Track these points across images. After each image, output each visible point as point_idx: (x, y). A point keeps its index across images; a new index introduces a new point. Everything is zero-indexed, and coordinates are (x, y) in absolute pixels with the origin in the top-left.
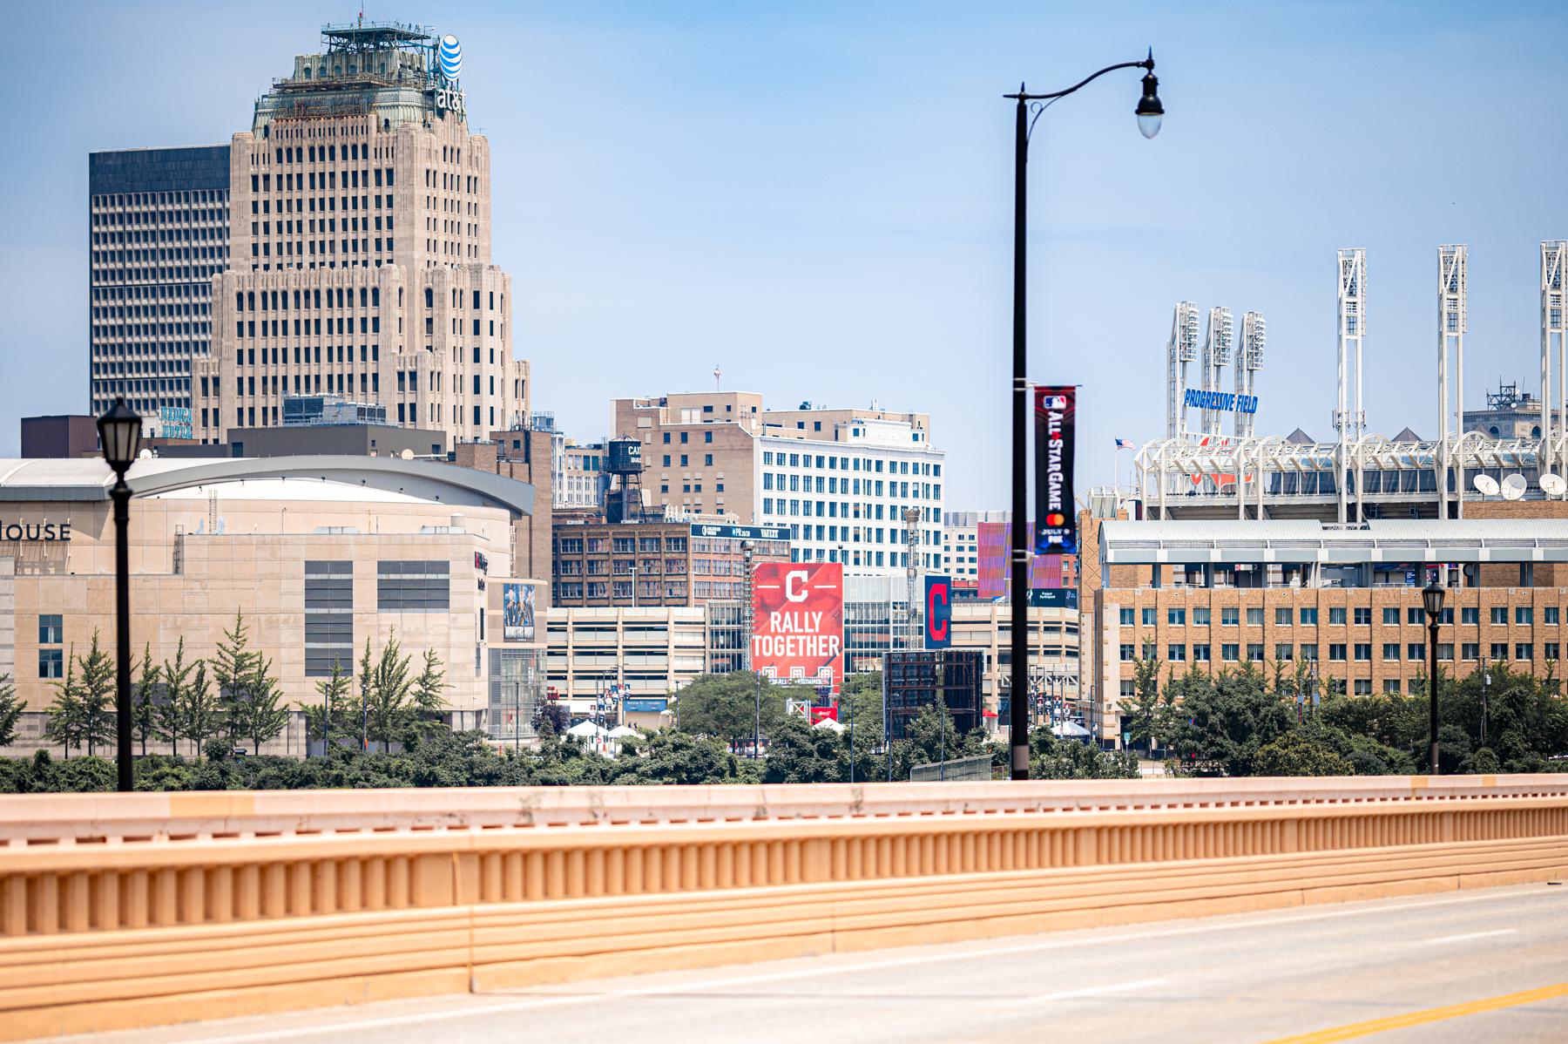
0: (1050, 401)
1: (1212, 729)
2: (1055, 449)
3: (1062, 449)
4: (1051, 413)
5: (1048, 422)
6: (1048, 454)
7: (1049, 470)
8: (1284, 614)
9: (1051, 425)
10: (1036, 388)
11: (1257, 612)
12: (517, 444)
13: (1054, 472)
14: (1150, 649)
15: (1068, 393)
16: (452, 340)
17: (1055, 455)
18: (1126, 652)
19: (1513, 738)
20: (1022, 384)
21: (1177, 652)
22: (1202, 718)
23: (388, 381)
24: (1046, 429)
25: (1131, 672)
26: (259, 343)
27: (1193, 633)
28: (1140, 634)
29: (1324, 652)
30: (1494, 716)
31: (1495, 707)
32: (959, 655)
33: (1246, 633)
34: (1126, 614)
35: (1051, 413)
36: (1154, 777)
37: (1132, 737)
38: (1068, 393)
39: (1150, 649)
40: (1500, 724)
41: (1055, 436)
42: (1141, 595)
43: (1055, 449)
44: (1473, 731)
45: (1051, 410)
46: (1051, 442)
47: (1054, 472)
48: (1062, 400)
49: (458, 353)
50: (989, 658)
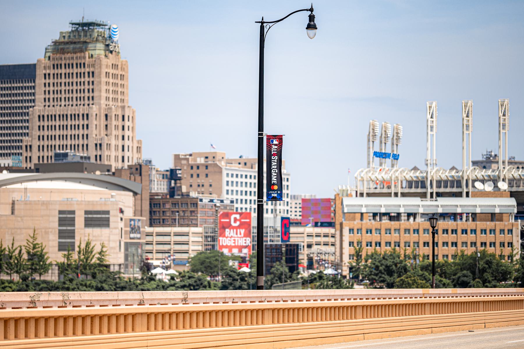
0: (273, 142)
1: (381, 272)
2: (275, 160)
8: (407, 231)
10: (267, 136)
11: (398, 230)
12: (137, 169)
13: (274, 169)
14: (359, 243)
15: (280, 138)
16: (114, 132)
17: (275, 162)
18: (351, 244)
19: (487, 276)
20: (262, 134)
21: (369, 244)
22: (377, 268)
23: (92, 147)
24: (271, 152)
25: (353, 252)
26: (46, 133)
27: (375, 237)
28: (356, 237)
29: (421, 244)
30: (481, 267)
31: (481, 264)
32: (291, 245)
33: (394, 237)
34: (351, 230)
35: (273, 146)
36: (359, 290)
37: (353, 275)
38: (280, 138)
39: (359, 243)
40: (483, 271)
41: (274, 155)
42: (356, 223)
43: (275, 160)
44: (473, 273)
45: (273, 145)
46: (273, 157)
47: (274, 169)
48: (277, 141)
49: (117, 137)
50: (303, 246)
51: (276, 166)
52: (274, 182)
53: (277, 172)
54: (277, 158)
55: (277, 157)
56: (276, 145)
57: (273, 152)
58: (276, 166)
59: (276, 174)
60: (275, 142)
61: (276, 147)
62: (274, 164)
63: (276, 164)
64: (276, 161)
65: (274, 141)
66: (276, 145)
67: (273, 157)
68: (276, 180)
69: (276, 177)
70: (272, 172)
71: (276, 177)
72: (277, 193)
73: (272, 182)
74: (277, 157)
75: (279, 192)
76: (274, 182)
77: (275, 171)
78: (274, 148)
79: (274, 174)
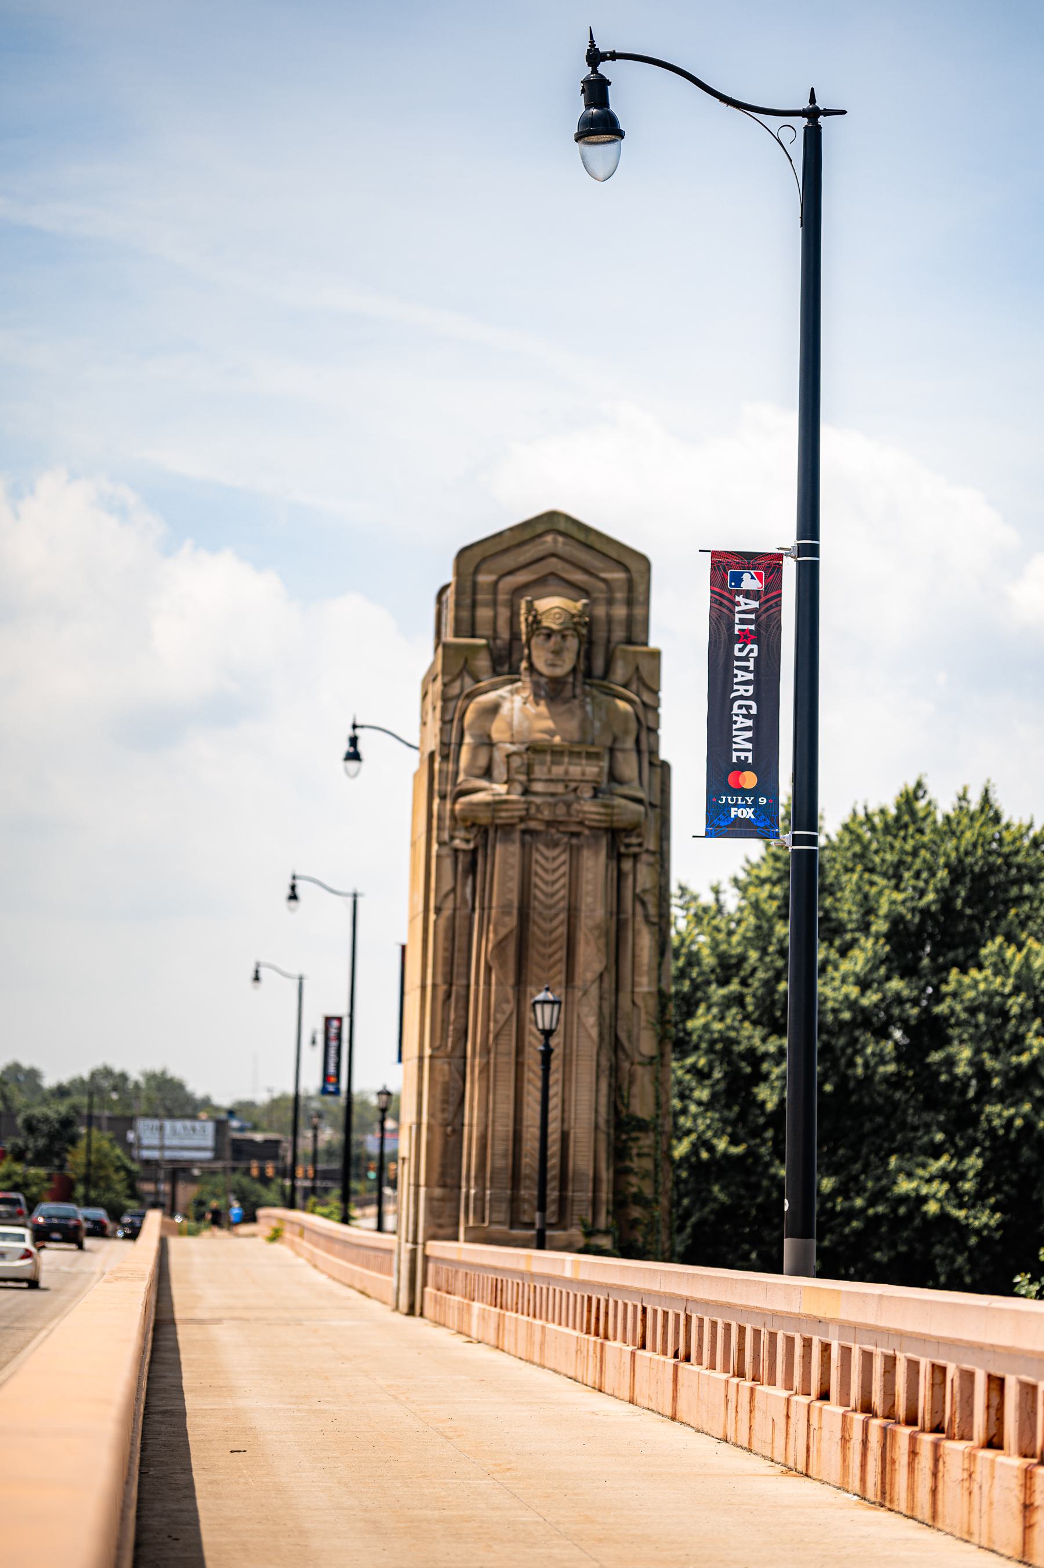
0: (738, 579)
2: (746, 659)
4: (739, 599)
5: (732, 612)
6: (733, 667)
9: (737, 617)
13: (742, 697)
17: (746, 669)
24: (731, 625)
35: (739, 599)
41: (745, 638)
43: (746, 659)
45: (739, 593)
46: (737, 646)
47: (742, 697)
51: (751, 688)
53: (754, 711)
54: (755, 654)
55: (755, 647)
56: (747, 594)
57: (737, 627)
58: (751, 688)
59: (749, 723)
60: (750, 582)
61: (755, 604)
62: (741, 676)
63: (750, 676)
64: (751, 664)
65: (746, 577)
66: (747, 594)
67: (737, 646)
68: (749, 746)
70: (735, 710)
72: (755, 803)
73: (735, 754)
74: (755, 647)
75: (763, 801)
76: (743, 755)
78: (743, 607)
79: (741, 722)
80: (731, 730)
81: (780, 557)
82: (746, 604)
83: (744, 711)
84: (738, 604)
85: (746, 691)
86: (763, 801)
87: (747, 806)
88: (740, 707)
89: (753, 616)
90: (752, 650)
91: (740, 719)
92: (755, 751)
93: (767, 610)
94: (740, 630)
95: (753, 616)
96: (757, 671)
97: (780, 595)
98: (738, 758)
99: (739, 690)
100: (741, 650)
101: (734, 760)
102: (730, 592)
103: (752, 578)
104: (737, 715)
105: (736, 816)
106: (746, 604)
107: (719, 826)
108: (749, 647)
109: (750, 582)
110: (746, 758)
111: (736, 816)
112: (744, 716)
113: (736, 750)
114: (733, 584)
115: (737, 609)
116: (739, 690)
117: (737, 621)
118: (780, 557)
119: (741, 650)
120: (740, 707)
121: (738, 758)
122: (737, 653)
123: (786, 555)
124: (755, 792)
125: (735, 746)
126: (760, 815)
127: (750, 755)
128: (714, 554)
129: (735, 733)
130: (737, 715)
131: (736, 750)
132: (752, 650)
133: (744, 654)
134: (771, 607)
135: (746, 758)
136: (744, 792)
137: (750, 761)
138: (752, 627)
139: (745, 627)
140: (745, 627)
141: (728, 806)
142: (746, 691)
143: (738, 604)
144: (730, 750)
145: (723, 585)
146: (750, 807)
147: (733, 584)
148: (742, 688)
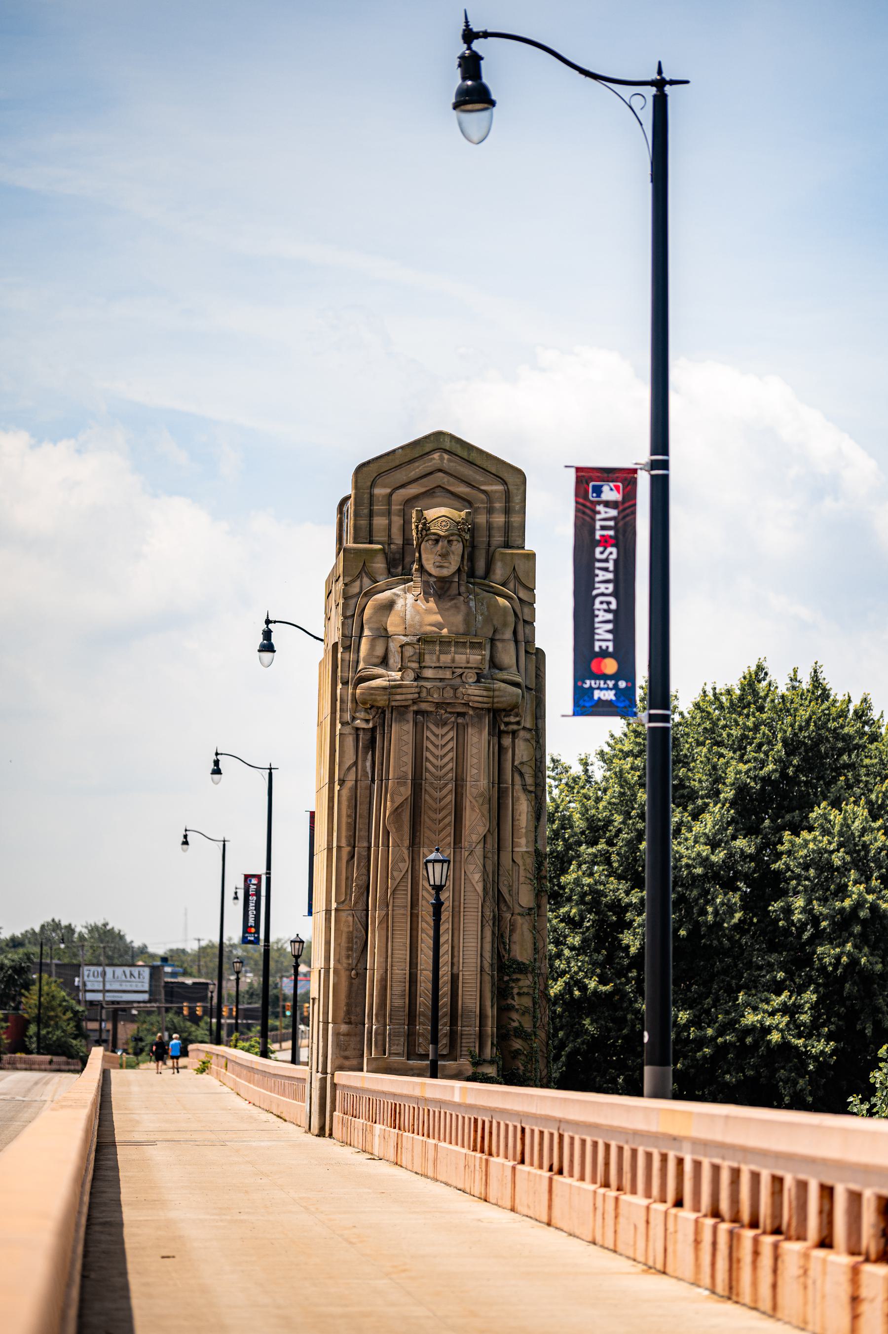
0: (598, 491)
2: (606, 560)
3: (616, 562)
4: (600, 508)
5: (594, 520)
6: (594, 568)
7: (595, 592)
9: (598, 524)
13: (603, 594)
17: (606, 569)
24: (593, 531)
35: (600, 508)
41: (605, 542)
43: (606, 560)
45: (599, 503)
46: (598, 550)
47: (603, 594)
48: (617, 488)
51: (611, 587)
52: (604, 645)
53: (613, 606)
54: (614, 556)
56: (607, 504)
59: (610, 616)
60: (610, 493)
61: (613, 513)
62: (602, 576)
63: (610, 576)
64: (611, 565)
65: (606, 489)
66: (607, 504)
68: (610, 636)
69: (610, 626)
70: (597, 605)
71: (610, 626)
72: (616, 686)
75: (622, 684)
77: (609, 603)
78: (603, 516)
79: (602, 616)
80: (593, 623)
81: (635, 471)
82: (606, 512)
83: (605, 606)
84: (599, 513)
85: (607, 588)
86: (622, 684)
87: (608, 689)
88: (602, 603)
89: (612, 523)
90: (611, 553)
91: (601, 613)
92: (615, 641)
93: (624, 518)
94: (601, 536)
95: (612, 523)
96: (616, 571)
97: (635, 505)
98: (600, 647)
99: (599, 588)
100: (602, 553)
101: (597, 649)
102: (592, 502)
103: (611, 489)
104: (599, 610)
105: (599, 698)
106: (606, 512)
107: (584, 707)
108: (609, 549)
109: (610, 493)
110: (607, 647)
111: (599, 698)
112: (605, 611)
113: (599, 640)
114: (595, 495)
115: (598, 517)
116: (599, 588)
117: (598, 527)
118: (635, 471)
119: (602, 553)
120: (602, 603)
121: (600, 647)
122: (598, 556)
123: (641, 469)
124: (616, 677)
125: (597, 637)
126: (620, 697)
127: (610, 645)
128: (578, 469)
129: (597, 625)
130: (599, 610)
131: (599, 640)
132: (611, 553)
133: (604, 556)
134: (627, 515)
135: (607, 647)
136: (606, 677)
137: (611, 649)
138: (611, 533)
139: (605, 533)
140: (605, 533)
141: (591, 689)
142: (607, 588)
143: (599, 513)
144: (592, 641)
145: (586, 497)
146: (611, 689)
147: (595, 495)
148: (603, 586)
